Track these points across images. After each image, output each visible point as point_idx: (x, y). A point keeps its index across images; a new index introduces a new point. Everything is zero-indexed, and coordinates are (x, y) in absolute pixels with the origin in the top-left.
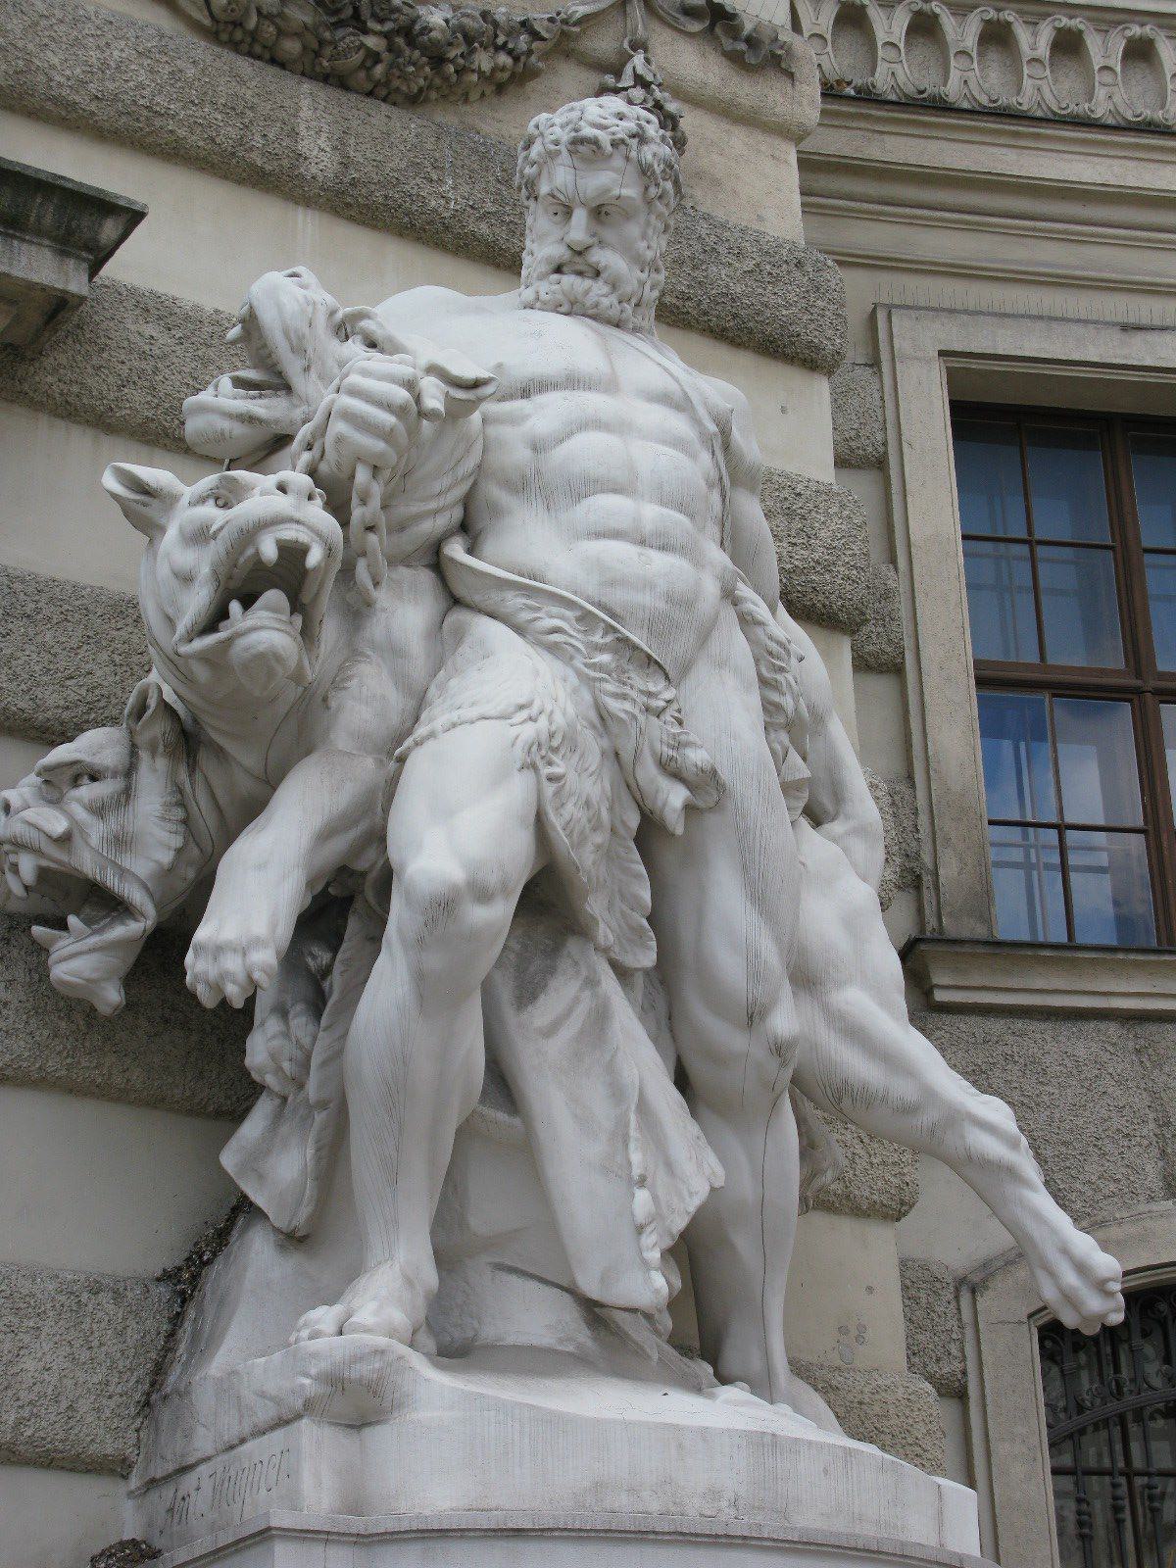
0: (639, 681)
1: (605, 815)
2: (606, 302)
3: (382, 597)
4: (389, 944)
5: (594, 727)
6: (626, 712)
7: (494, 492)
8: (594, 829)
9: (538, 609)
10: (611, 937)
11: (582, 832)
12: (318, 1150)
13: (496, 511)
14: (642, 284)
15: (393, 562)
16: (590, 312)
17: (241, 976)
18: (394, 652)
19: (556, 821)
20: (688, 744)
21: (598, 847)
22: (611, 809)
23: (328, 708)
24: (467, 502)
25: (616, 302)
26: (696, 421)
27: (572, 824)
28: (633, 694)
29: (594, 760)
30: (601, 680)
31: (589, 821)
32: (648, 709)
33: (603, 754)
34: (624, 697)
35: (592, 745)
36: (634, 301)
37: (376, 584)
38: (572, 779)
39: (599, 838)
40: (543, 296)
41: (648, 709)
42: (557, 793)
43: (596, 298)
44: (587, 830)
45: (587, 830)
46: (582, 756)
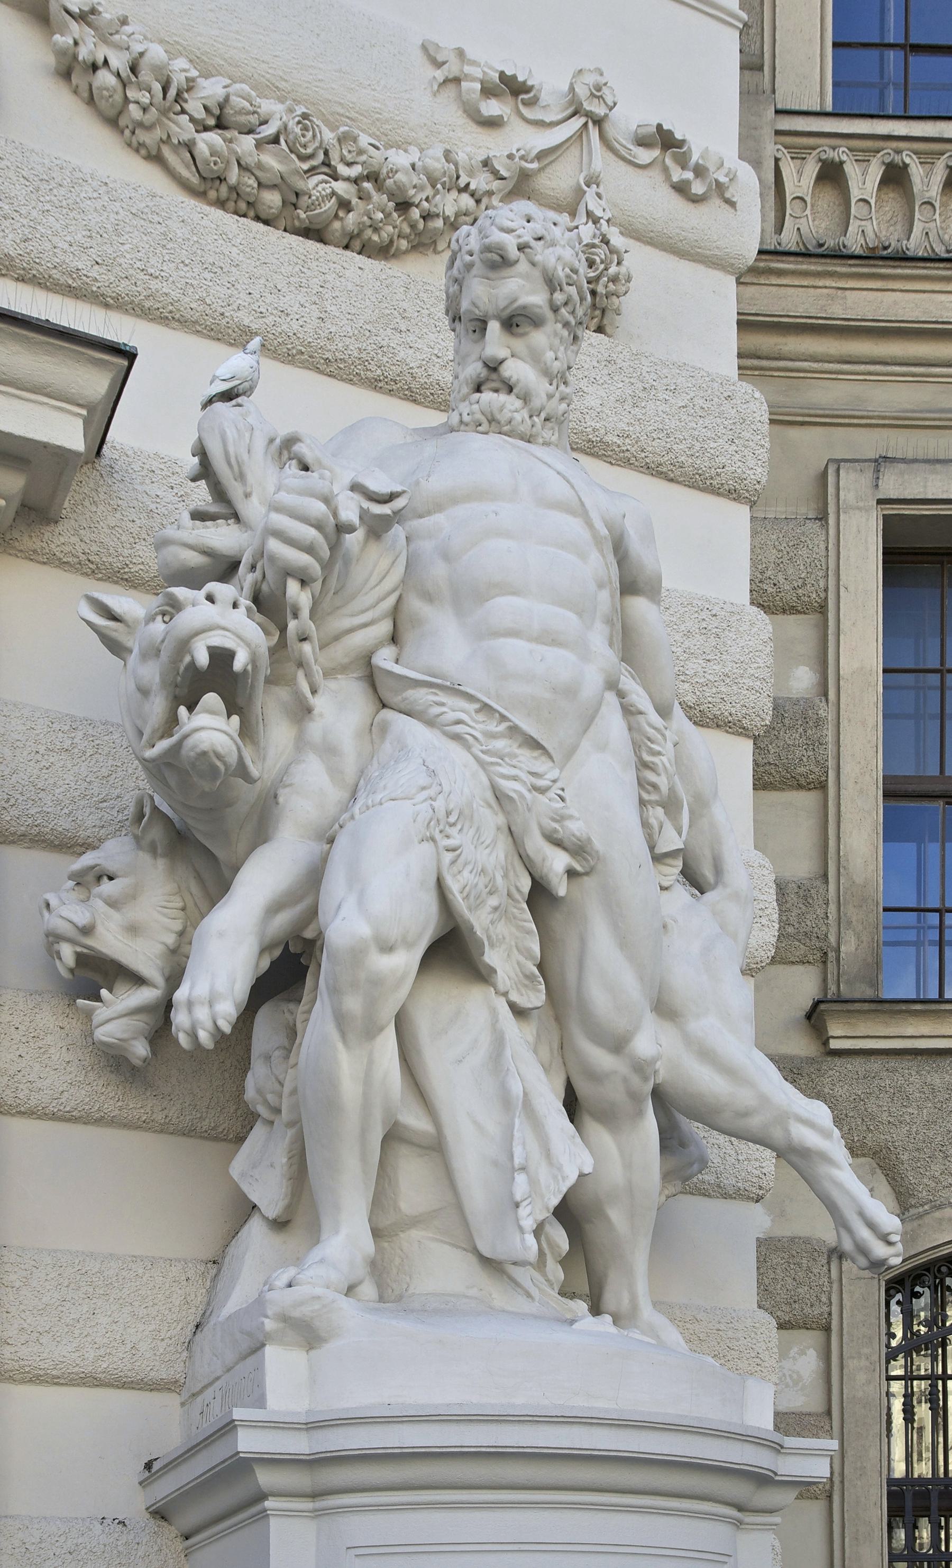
0: (527, 759)
1: (499, 880)
2: (518, 417)
3: (319, 703)
4: (321, 994)
5: (490, 806)
6: (515, 791)
7: (415, 604)
8: (491, 893)
9: (443, 704)
10: (508, 982)
11: (478, 897)
12: (290, 1158)
13: (417, 622)
14: (550, 396)
15: (329, 673)
16: (506, 428)
17: (209, 1025)
18: (329, 751)
19: (454, 886)
20: (571, 817)
21: (496, 909)
22: (505, 876)
23: (277, 803)
24: (395, 613)
25: (527, 417)
26: (589, 524)
27: (467, 889)
28: (523, 776)
29: (489, 834)
30: (492, 763)
31: (486, 887)
32: (536, 789)
33: (498, 829)
34: (515, 778)
35: (491, 820)
36: (543, 415)
37: (314, 692)
38: (468, 852)
39: (493, 901)
40: (466, 418)
41: (536, 789)
42: (453, 862)
43: (510, 414)
44: (484, 895)
45: (484, 895)
46: (478, 829)
